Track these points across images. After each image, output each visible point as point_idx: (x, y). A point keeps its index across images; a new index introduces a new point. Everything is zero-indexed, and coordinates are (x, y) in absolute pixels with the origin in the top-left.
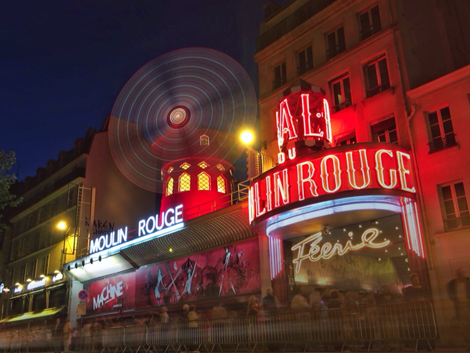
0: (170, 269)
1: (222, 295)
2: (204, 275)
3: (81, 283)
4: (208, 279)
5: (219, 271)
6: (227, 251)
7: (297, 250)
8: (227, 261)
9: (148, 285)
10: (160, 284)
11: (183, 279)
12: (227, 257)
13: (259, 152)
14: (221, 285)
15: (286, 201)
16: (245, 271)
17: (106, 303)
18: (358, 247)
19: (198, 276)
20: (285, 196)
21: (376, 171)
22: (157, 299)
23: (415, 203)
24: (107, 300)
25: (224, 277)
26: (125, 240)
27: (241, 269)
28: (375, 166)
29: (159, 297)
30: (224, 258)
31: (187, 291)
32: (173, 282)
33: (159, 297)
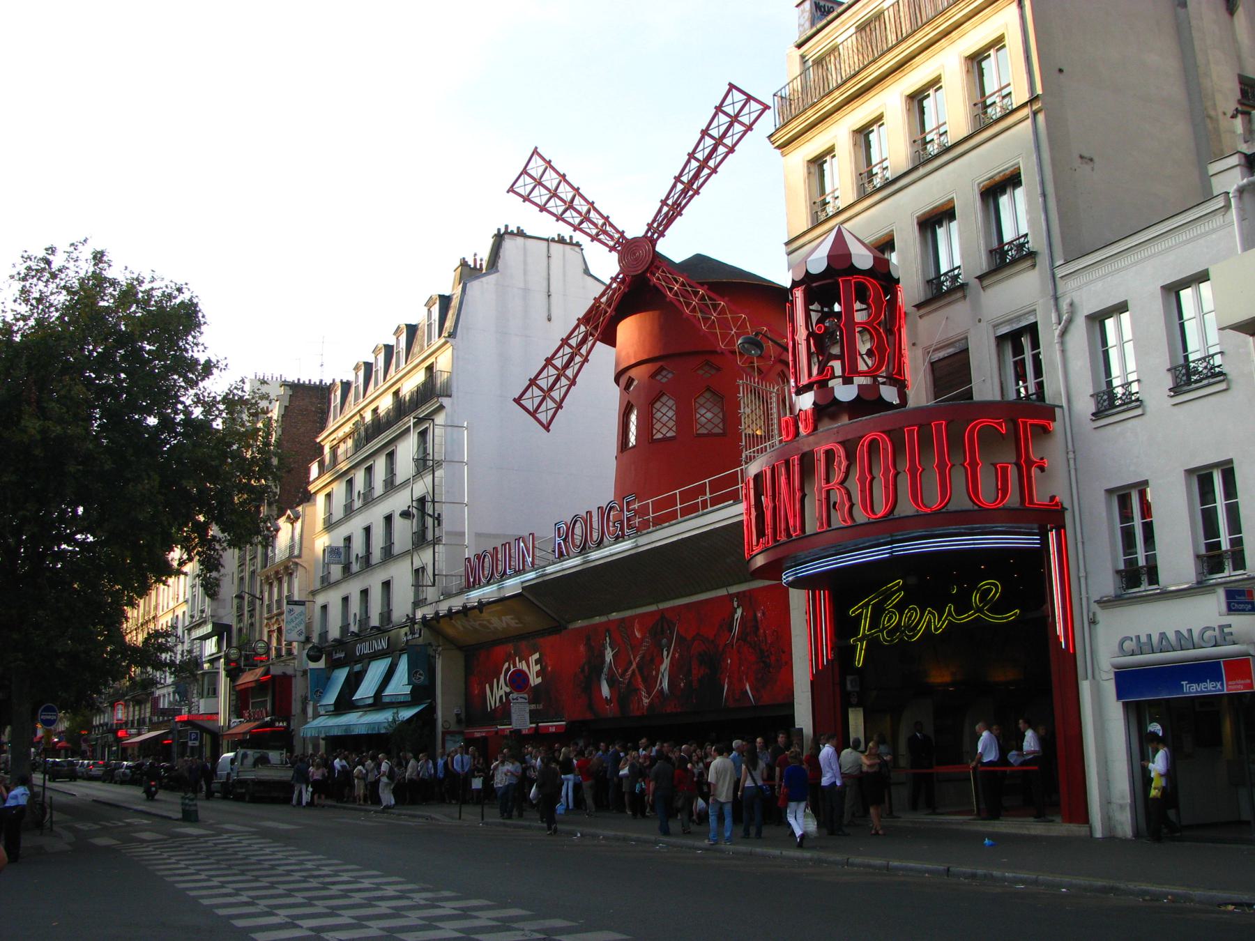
3: (460, 648)
6: (735, 604)
7: (859, 616)
9: (586, 667)
10: (610, 668)
13: (778, 384)
18: (965, 618)
32: (634, 666)
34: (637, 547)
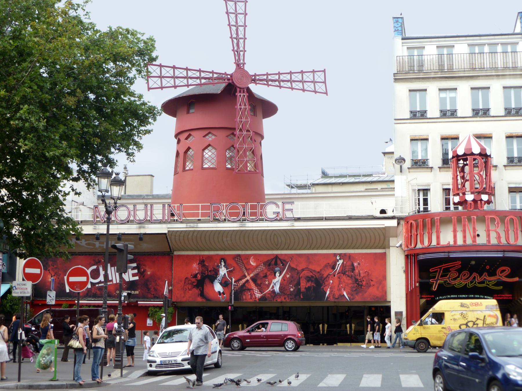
0: (243, 263)
1: (329, 299)
2: (301, 277)
4: (308, 281)
5: (325, 276)
6: (338, 258)
8: (338, 268)
11: (266, 276)
12: (338, 263)
14: (329, 289)
16: (363, 281)
17: (97, 285)
19: (292, 277)
22: (218, 294)
24: (100, 282)
25: (332, 283)
27: (358, 277)
29: (222, 292)
30: (334, 264)
31: (274, 290)
32: (248, 278)
33: (222, 292)
34: (293, 226)
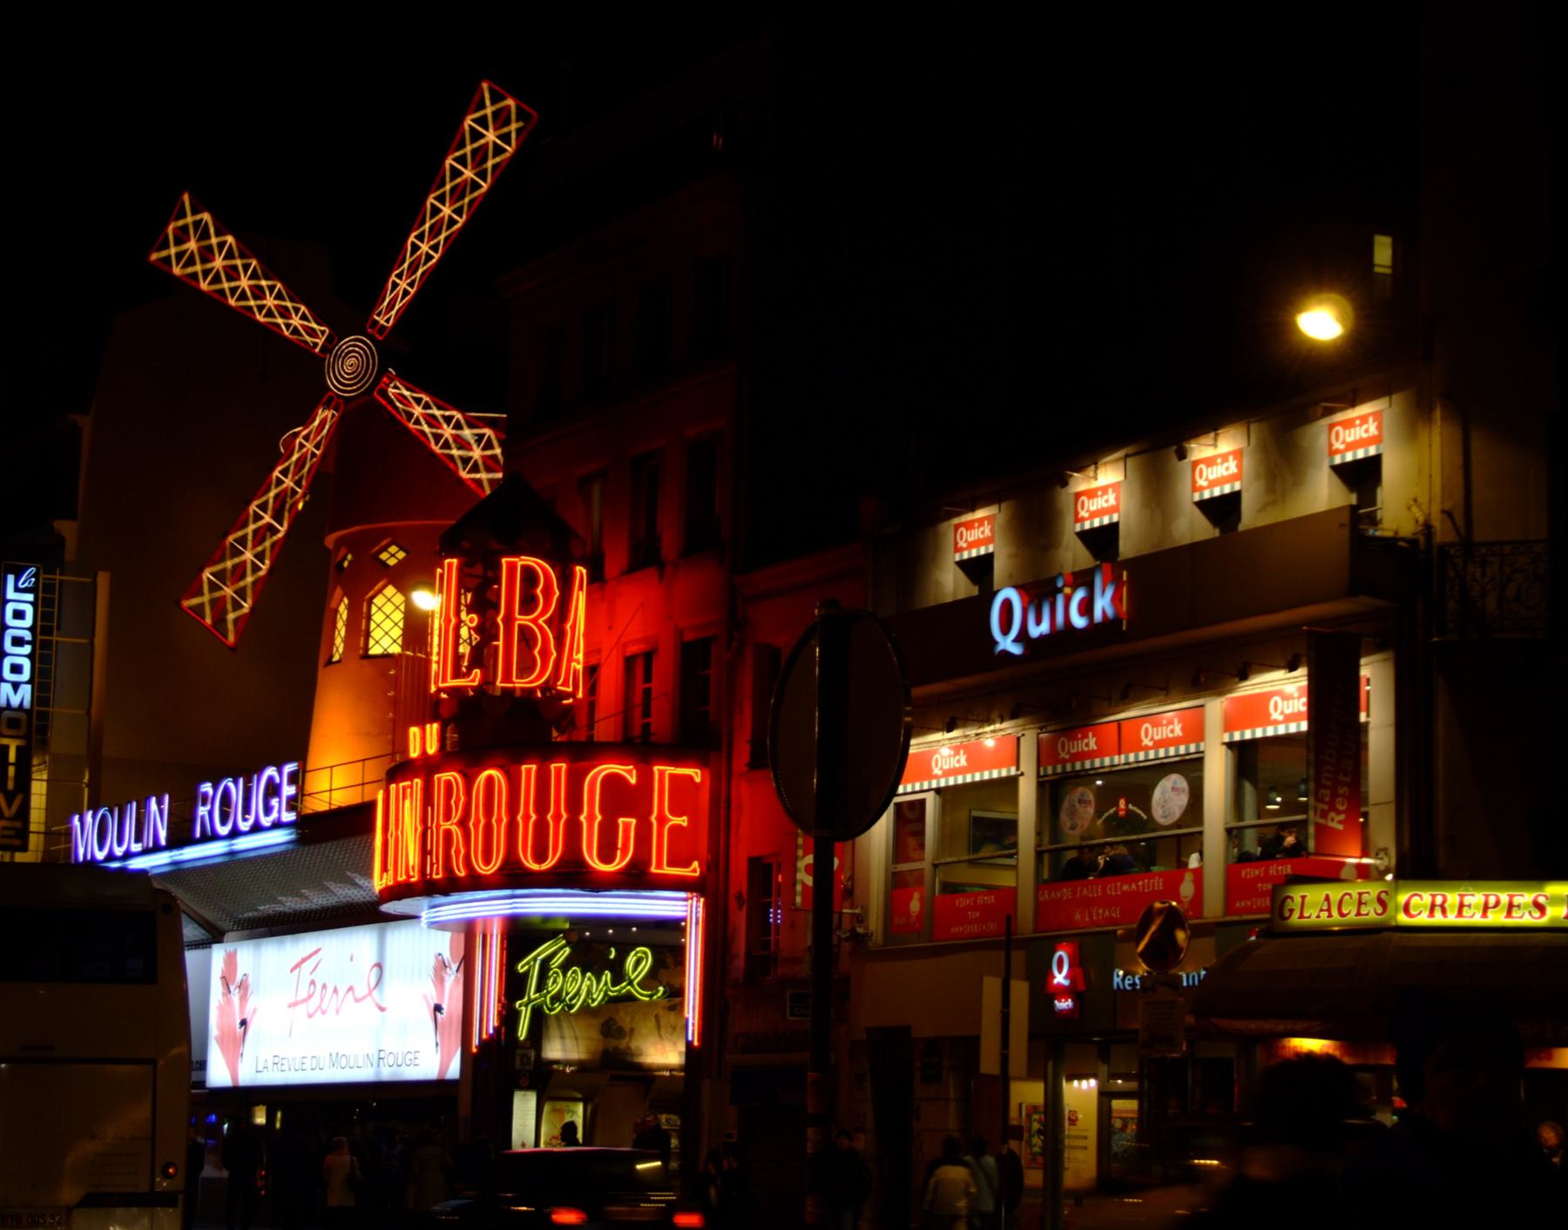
15: (413, 868)
20: (413, 857)
21: (580, 824)
23: (702, 900)
26: (163, 842)
28: (580, 811)
